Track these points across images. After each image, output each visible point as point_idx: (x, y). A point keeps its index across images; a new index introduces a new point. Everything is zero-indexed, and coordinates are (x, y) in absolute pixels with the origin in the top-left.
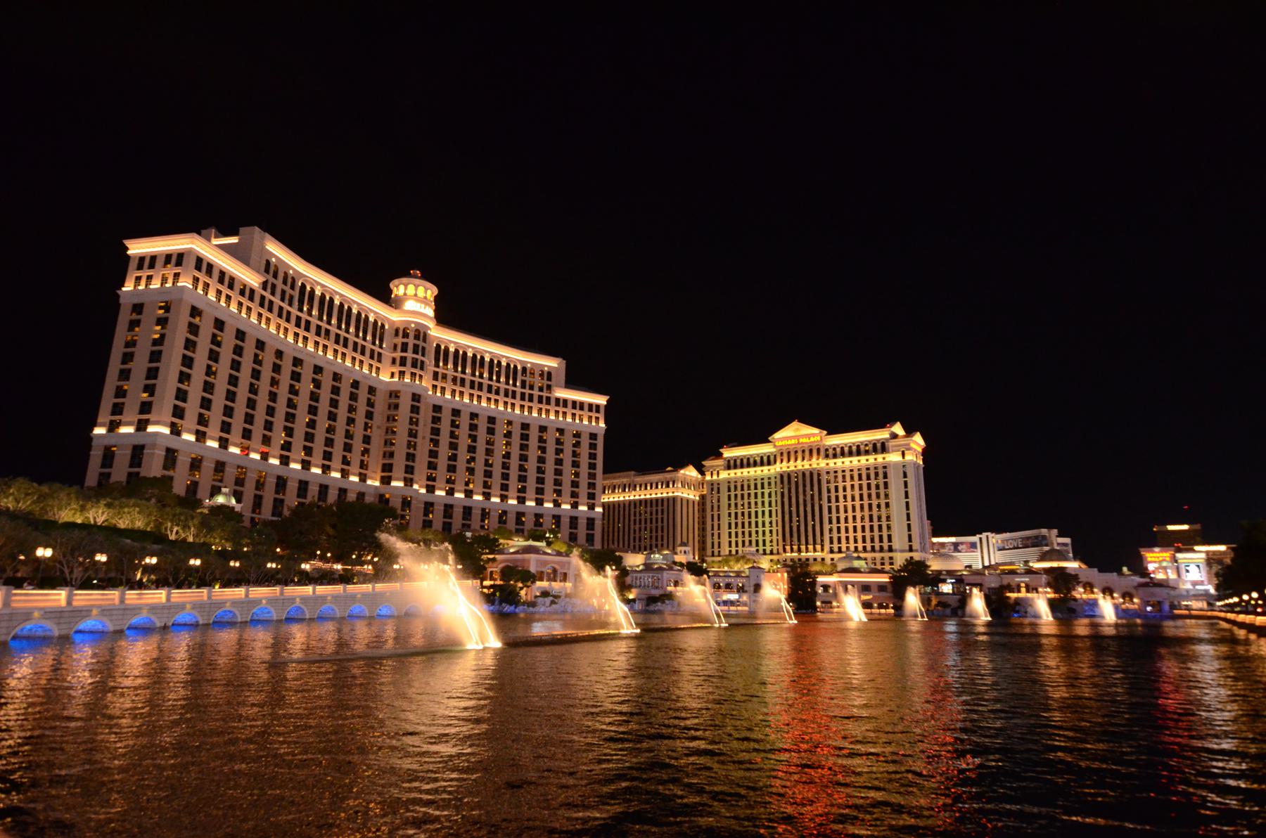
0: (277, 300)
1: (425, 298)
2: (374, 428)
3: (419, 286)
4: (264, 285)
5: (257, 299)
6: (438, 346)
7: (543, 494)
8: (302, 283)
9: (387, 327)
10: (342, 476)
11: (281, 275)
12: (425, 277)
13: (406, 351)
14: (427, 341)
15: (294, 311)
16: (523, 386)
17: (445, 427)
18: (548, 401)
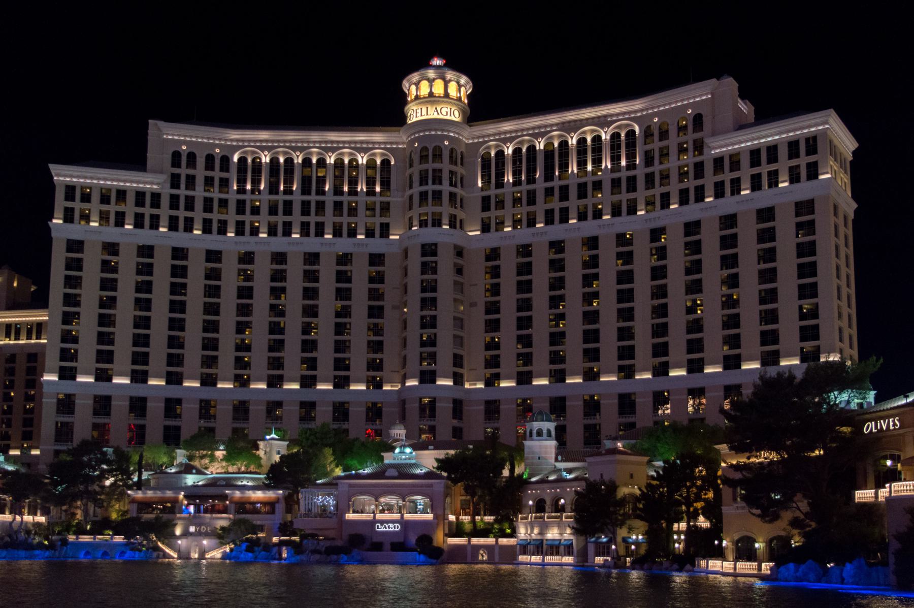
0: (199, 193)
1: (431, 94)
2: (387, 312)
3: (419, 82)
4: (175, 181)
5: (165, 202)
7: (701, 350)
8: (240, 159)
9: (393, 163)
10: (455, 383)
11: (201, 162)
12: (455, 64)
13: (440, 183)
14: (446, 155)
15: (232, 196)
16: (649, 160)
18: (699, 169)
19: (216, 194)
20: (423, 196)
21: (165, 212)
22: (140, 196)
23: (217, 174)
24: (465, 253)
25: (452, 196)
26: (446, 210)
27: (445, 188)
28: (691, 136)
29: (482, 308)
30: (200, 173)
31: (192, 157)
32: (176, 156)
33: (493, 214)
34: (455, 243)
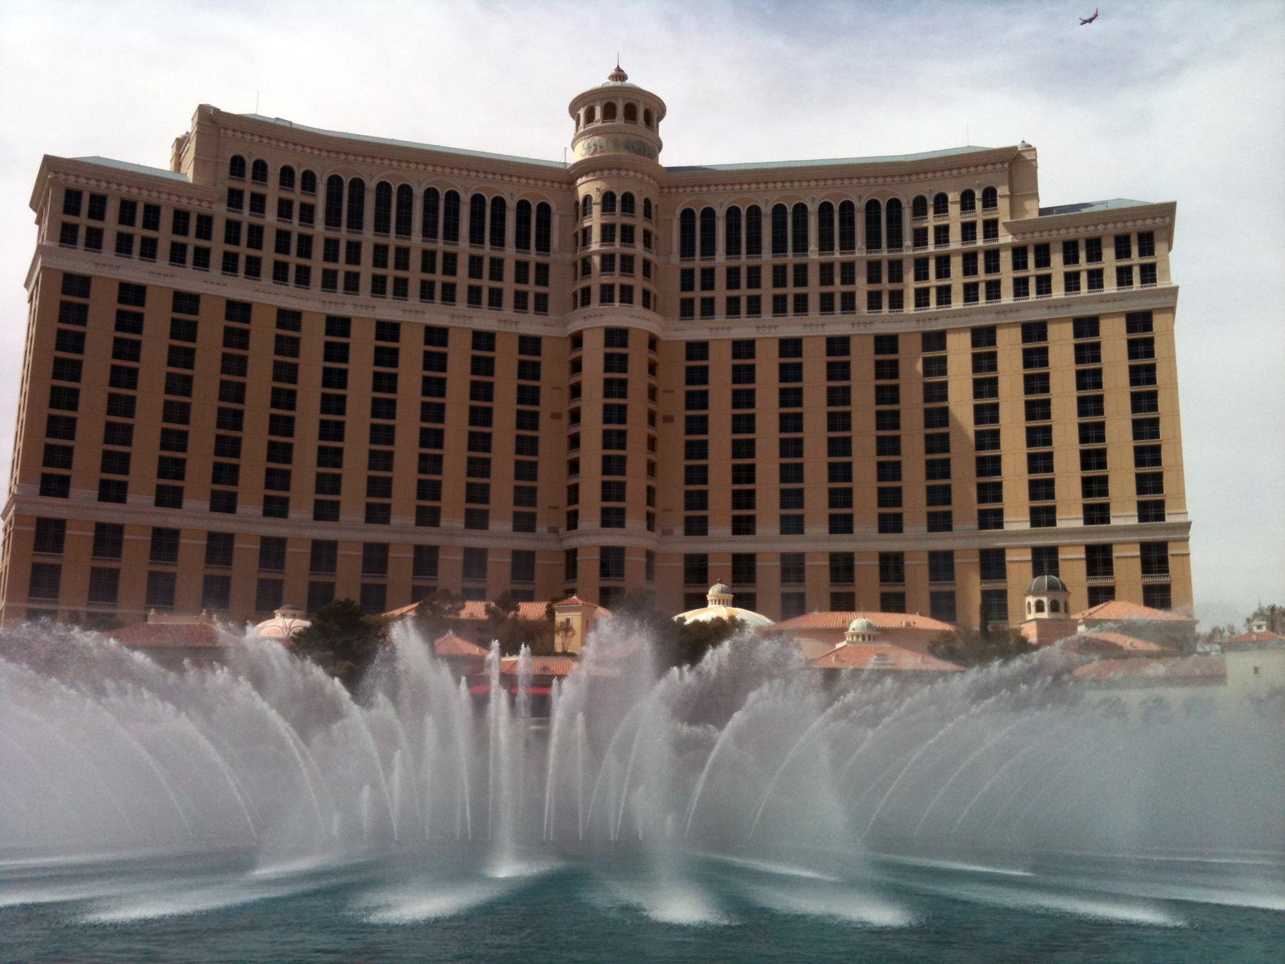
2: (544, 420)
4: (234, 199)
5: (219, 230)
6: (687, 215)
9: (553, 207)
17: (720, 386)
19: (295, 226)
20: (608, 261)
21: (217, 245)
22: (181, 219)
23: (297, 196)
24: (659, 346)
25: (647, 265)
26: (637, 281)
27: (638, 249)
28: (979, 215)
29: (680, 424)
30: (273, 191)
31: (260, 170)
32: (237, 165)
33: (698, 294)
34: (653, 331)
